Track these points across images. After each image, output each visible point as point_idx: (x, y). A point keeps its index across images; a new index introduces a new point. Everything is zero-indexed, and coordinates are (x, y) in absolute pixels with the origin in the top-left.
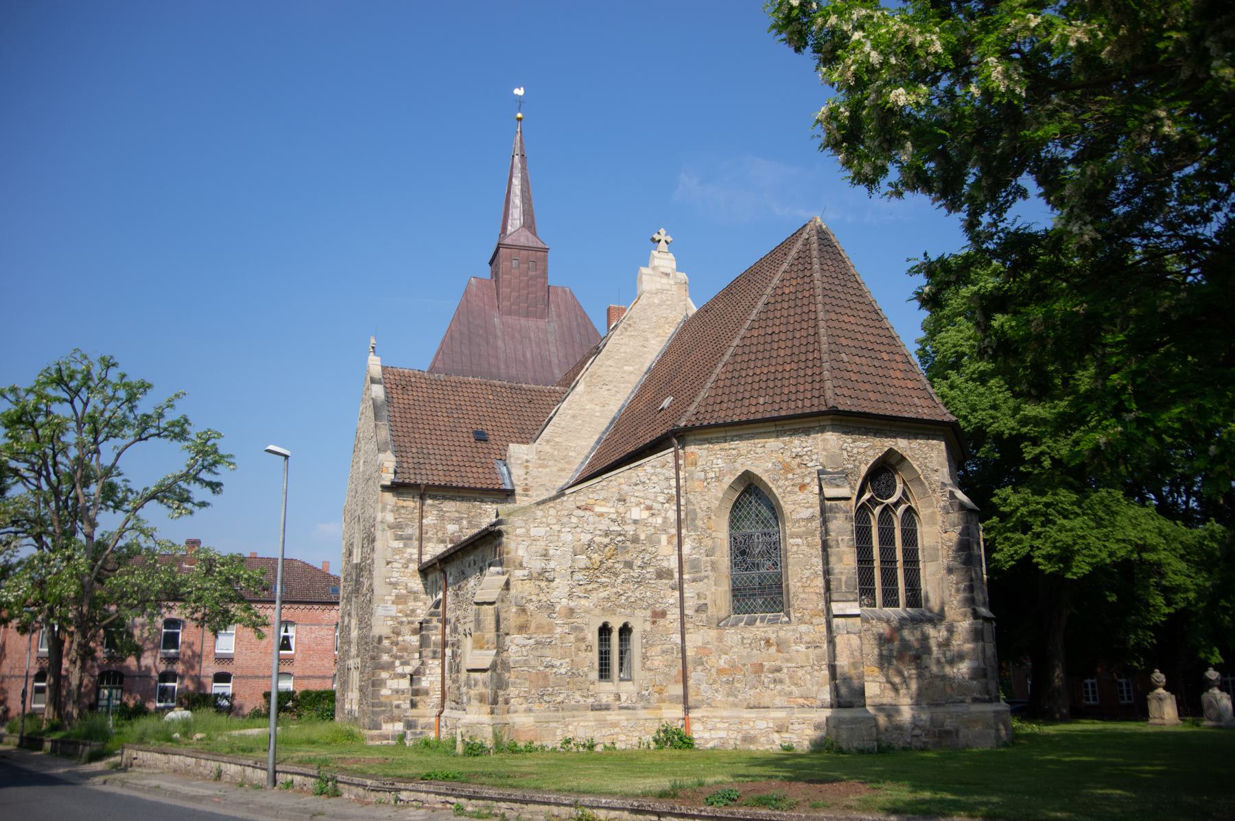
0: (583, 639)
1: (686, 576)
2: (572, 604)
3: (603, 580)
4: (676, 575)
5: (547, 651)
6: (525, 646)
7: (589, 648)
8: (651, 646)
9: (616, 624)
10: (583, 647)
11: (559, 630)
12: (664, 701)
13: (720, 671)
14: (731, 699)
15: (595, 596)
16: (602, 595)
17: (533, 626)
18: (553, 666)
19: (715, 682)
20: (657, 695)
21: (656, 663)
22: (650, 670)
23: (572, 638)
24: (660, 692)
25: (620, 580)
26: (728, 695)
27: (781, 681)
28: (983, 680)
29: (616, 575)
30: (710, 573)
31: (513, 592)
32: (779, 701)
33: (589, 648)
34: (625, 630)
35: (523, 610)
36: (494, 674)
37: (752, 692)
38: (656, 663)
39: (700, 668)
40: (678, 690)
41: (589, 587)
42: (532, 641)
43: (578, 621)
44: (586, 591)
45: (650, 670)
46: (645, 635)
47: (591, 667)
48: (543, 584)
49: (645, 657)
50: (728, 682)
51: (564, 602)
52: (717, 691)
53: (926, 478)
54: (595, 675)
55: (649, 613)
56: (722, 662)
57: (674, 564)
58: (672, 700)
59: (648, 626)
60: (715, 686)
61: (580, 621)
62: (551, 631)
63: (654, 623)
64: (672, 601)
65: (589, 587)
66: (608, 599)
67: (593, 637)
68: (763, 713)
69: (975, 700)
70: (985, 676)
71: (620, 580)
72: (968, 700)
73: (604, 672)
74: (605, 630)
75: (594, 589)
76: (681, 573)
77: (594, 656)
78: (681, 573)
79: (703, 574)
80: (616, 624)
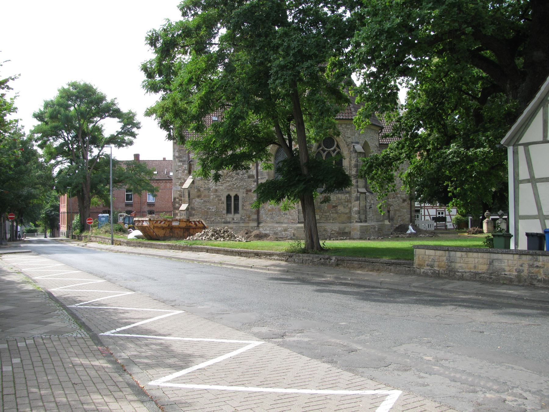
0: (221, 200)
1: (259, 177)
2: (216, 188)
3: (228, 179)
4: (255, 177)
5: (208, 204)
6: (200, 202)
7: (223, 203)
8: (246, 202)
9: (233, 194)
10: (221, 202)
11: (212, 197)
12: (250, 221)
13: (269, 210)
14: (272, 220)
15: (225, 185)
16: (227, 185)
17: (203, 195)
18: (210, 209)
19: (267, 214)
20: (248, 219)
21: (247, 208)
22: (245, 210)
23: (216, 199)
24: (249, 217)
25: (234, 179)
26: (271, 219)
27: (286, 214)
28: (359, 215)
29: (233, 178)
30: (266, 176)
31: (196, 184)
32: (286, 221)
33: (223, 203)
34: (236, 197)
35: (199, 190)
36: (188, 212)
37: (278, 218)
38: (247, 208)
39: (263, 209)
40: (255, 217)
41: (223, 182)
42: (202, 201)
43: (218, 194)
44: (222, 183)
45: (245, 210)
46: (243, 198)
47: (224, 209)
48: (206, 182)
49: (243, 206)
50: (271, 214)
51: (214, 187)
52: (268, 217)
53: (344, 140)
54: (225, 212)
55: (245, 190)
56: (269, 207)
57: (254, 173)
58: (253, 220)
59: (245, 195)
60: (267, 216)
61: (219, 193)
62: (209, 196)
63: (247, 194)
64: (253, 186)
65: (223, 182)
66: (230, 186)
67: (224, 199)
68: (280, 225)
69: (356, 222)
70: (359, 213)
71: (234, 179)
72: (355, 222)
73: (228, 211)
74: (229, 197)
75: (224, 183)
76: (257, 176)
77: (225, 205)
78: (257, 176)
79: (264, 176)
80: (233, 194)
